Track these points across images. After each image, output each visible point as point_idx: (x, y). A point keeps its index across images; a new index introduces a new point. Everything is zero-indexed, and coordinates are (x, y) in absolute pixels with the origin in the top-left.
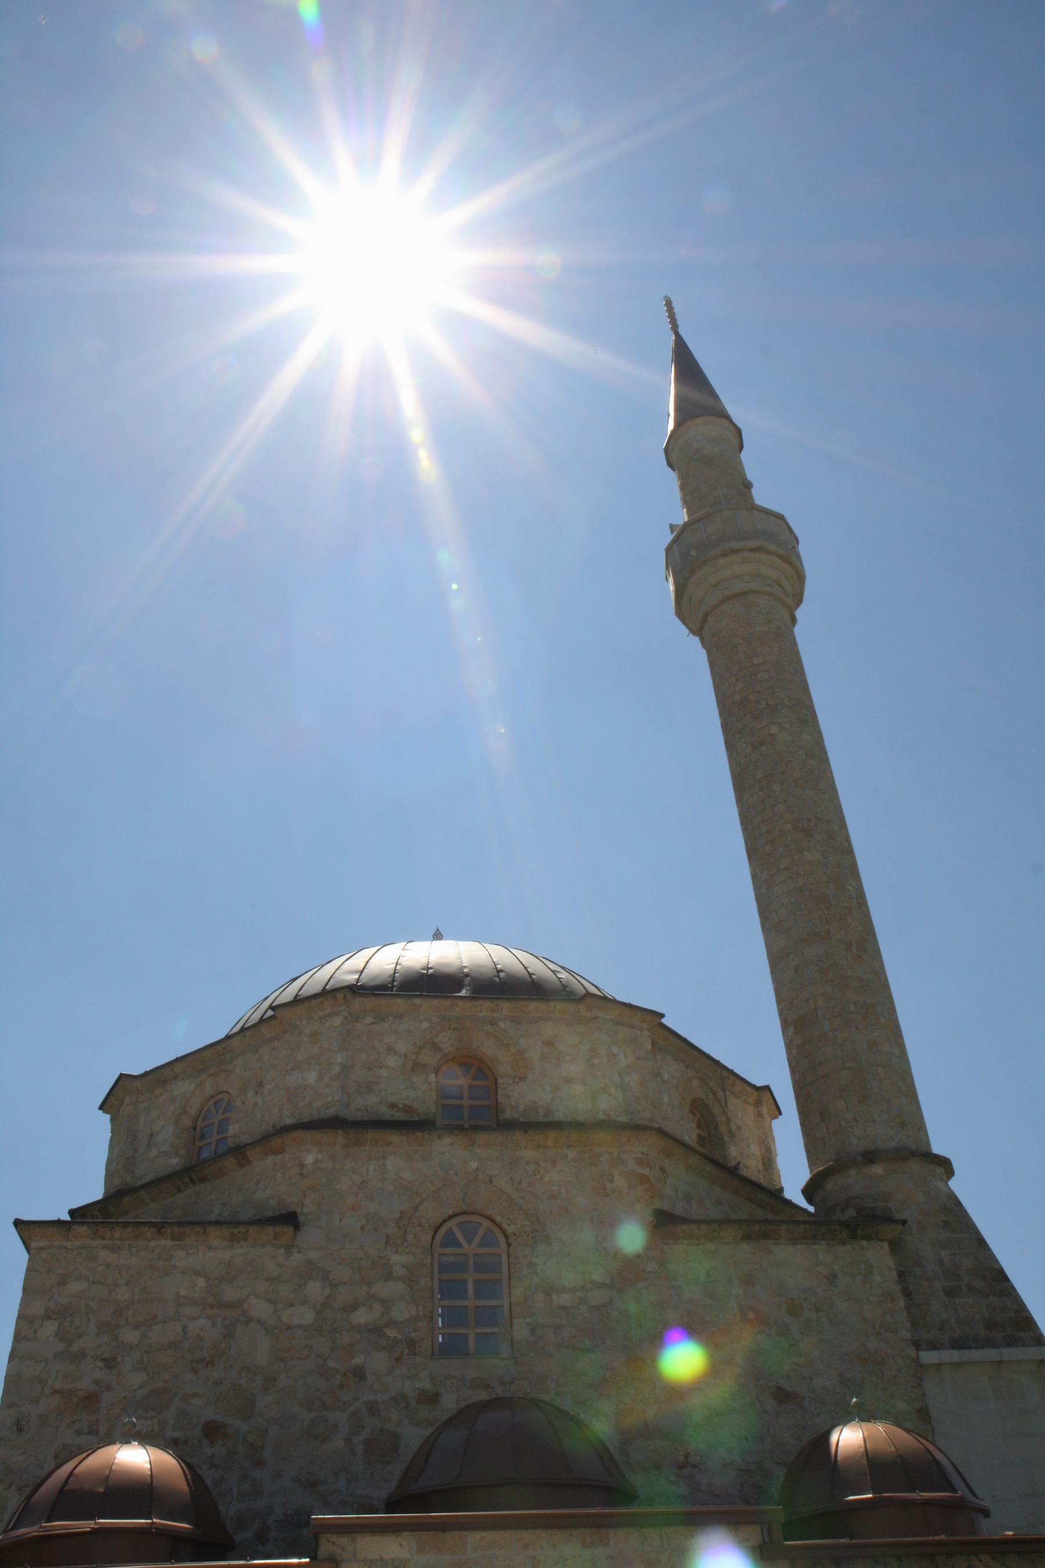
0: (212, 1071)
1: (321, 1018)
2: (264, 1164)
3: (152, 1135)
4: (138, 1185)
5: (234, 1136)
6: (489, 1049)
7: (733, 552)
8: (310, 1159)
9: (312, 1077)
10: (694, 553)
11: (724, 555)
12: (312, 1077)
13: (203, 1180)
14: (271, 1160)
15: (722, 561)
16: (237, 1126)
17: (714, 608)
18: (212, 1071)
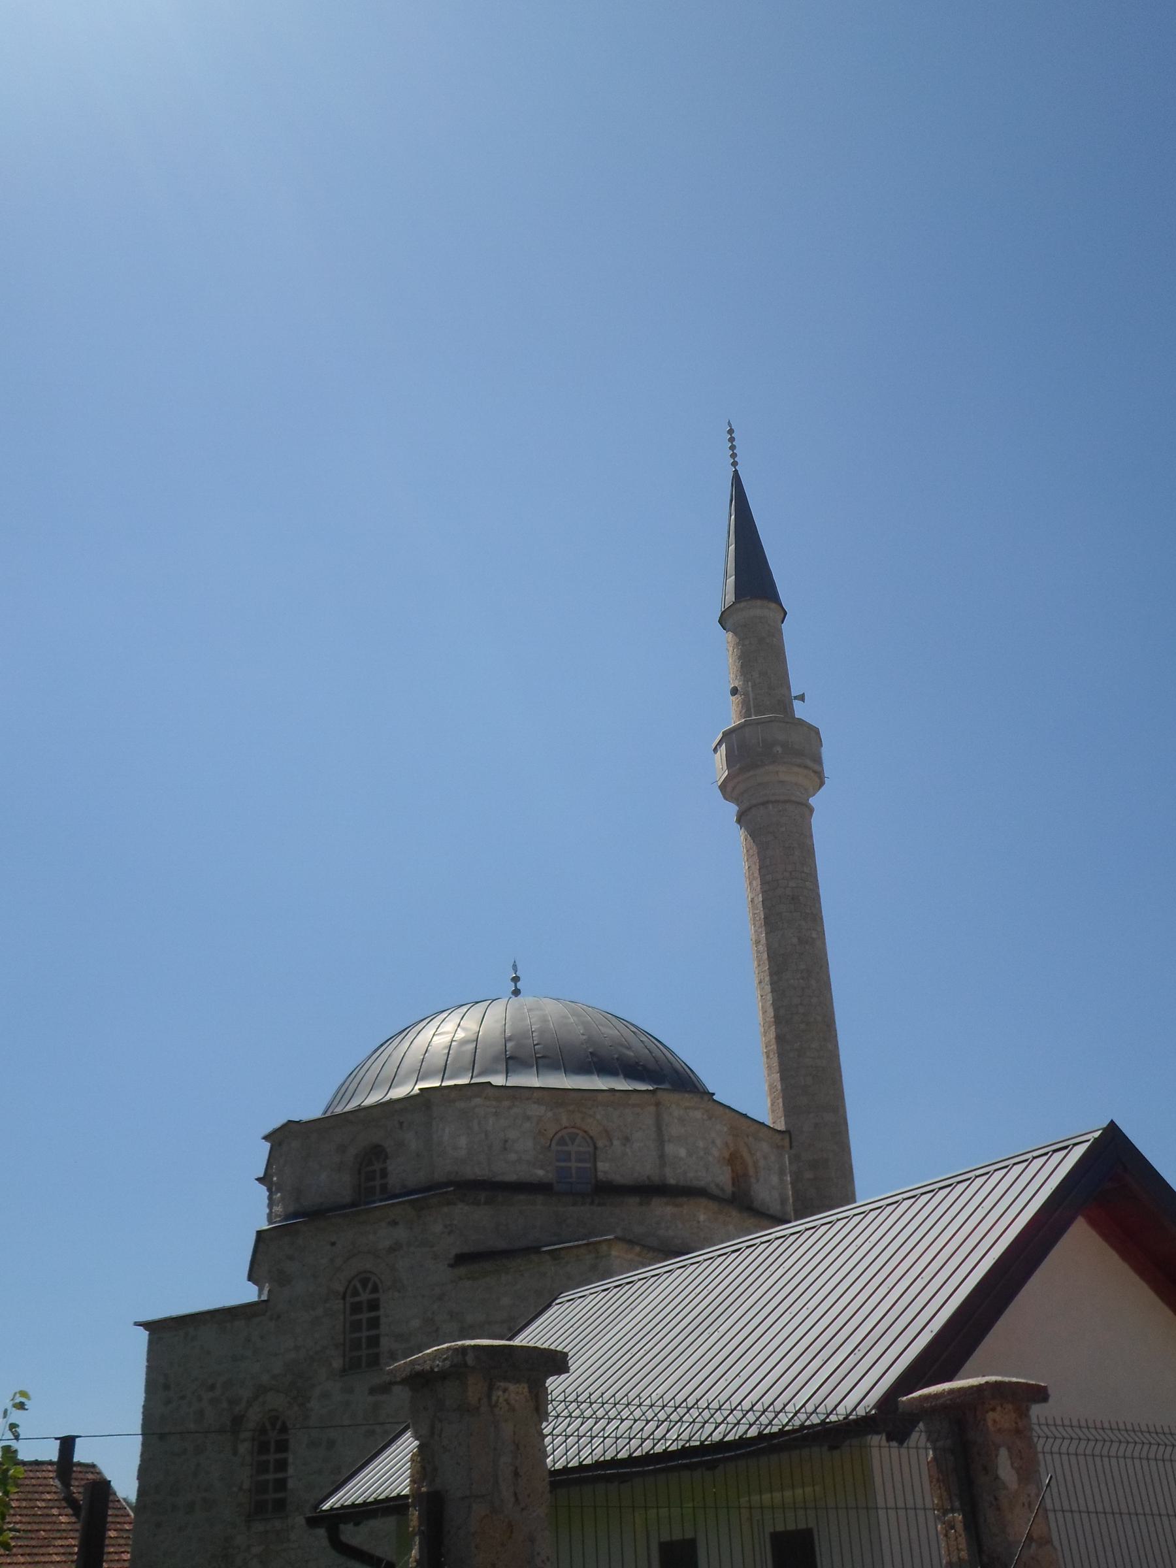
0: (571, 1108)
1: (686, 1108)
2: (661, 1209)
3: (506, 1141)
4: (498, 1179)
5: (605, 1173)
6: (745, 1153)
7: (806, 767)
8: (702, 1218)
9: (683, 1152)
10: (779, 749)
11: (799, 766)
12: (683, 1152)
13: (599, 1205)
14: (669, 1210)
15: (796, 769)
16: (607, 1165)
17: (777, 802)
18: (571, 1108)
